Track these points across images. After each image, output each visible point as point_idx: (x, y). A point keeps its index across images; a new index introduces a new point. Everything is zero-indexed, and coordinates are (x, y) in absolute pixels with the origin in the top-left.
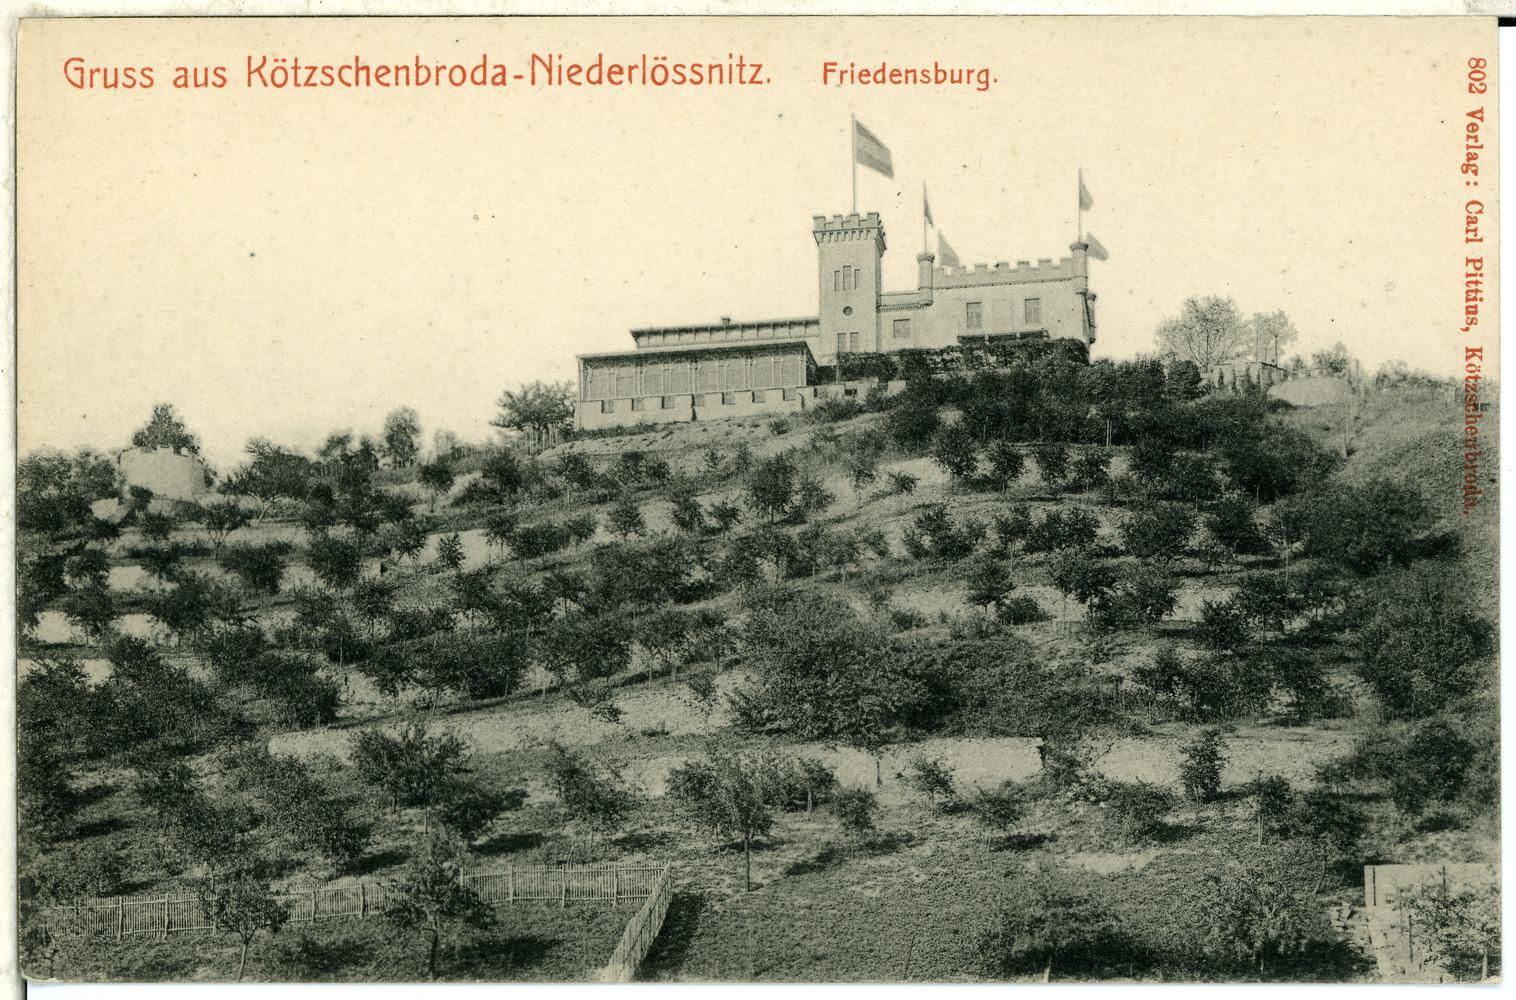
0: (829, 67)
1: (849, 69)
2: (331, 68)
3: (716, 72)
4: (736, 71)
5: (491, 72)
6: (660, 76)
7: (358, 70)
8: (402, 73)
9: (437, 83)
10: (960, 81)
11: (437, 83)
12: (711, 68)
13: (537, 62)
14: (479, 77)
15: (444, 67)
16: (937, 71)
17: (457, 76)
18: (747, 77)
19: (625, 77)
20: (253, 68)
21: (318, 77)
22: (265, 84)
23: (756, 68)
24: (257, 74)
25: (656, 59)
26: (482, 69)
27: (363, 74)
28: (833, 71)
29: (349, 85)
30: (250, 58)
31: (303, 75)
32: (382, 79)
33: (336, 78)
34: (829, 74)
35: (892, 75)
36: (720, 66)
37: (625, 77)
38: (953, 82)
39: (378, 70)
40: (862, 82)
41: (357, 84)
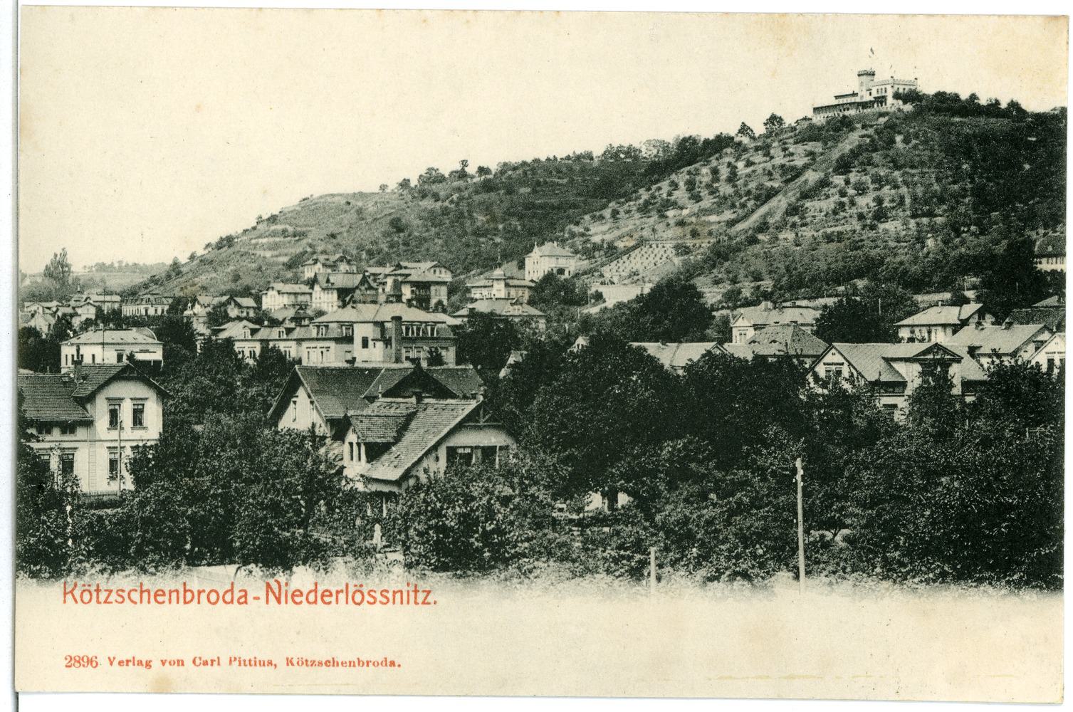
2: (123, 591)
3: (398, 596)
4: (412, 594)
5: (237, 595)
7: (142, 592)
8: (174, 595)
9: (199, 602)
11: (199, 602)
14: (228, 598)
15: (204, 591)
17: (213, 597)
18: (420, 600)
19: (333, 599)
23: (425, 594)
26: (230, 594)
27: (145, 595)
29: (135, 603)
37: (333, 599)
40: (325, 603)
41: (141, 602)
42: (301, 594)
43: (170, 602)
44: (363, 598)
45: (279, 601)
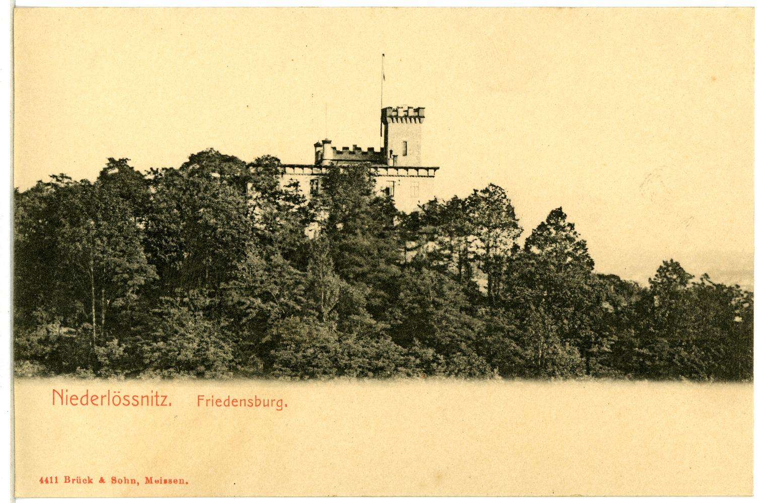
0: (200, 398)
1: (211, 398)
3: (145, 399)
4: (155, 398)
6: (117, 402)
10: (268, 405)
12: (142, 397)
13: (55, 393)
16: (256, 400)
18: (159, 403)
23: (164, 398)
25: (115, 392)
28: (203, 399)
34: (200, 401)
35: (233, 401)
36: (147, 396)
38: (264, 406)
42: (77, 399)
44: (120, 402)
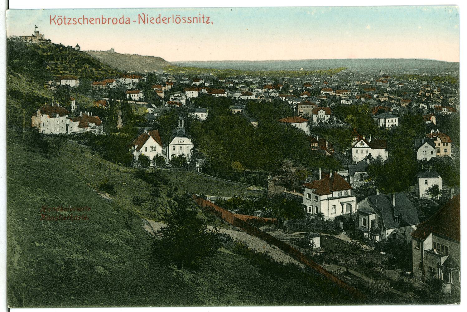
2: (76, 19)
3: (195, 19)
4: (202, 19)
5: (125, 20)
7: (84, 19)
8: (98, 20)
9: (109, 23)
11: (109, 23)
12: (194, 18)
14: (121, 21)
15: (111, 18)
17: (115, 21)
18: (205, 21)
20: (52, 18)
21: (72, 22)
22: (56, 24)
24: (53, 20)
27: (86, 20)
29: (81, 24)
30: (51, 16)
31: (67, 21)
32: (164, 21)
33: (77, 22)
36: (197, 18)
39: (90, 19)
41: (84, 23)
43: (96, 23)
45: (144, 22)
